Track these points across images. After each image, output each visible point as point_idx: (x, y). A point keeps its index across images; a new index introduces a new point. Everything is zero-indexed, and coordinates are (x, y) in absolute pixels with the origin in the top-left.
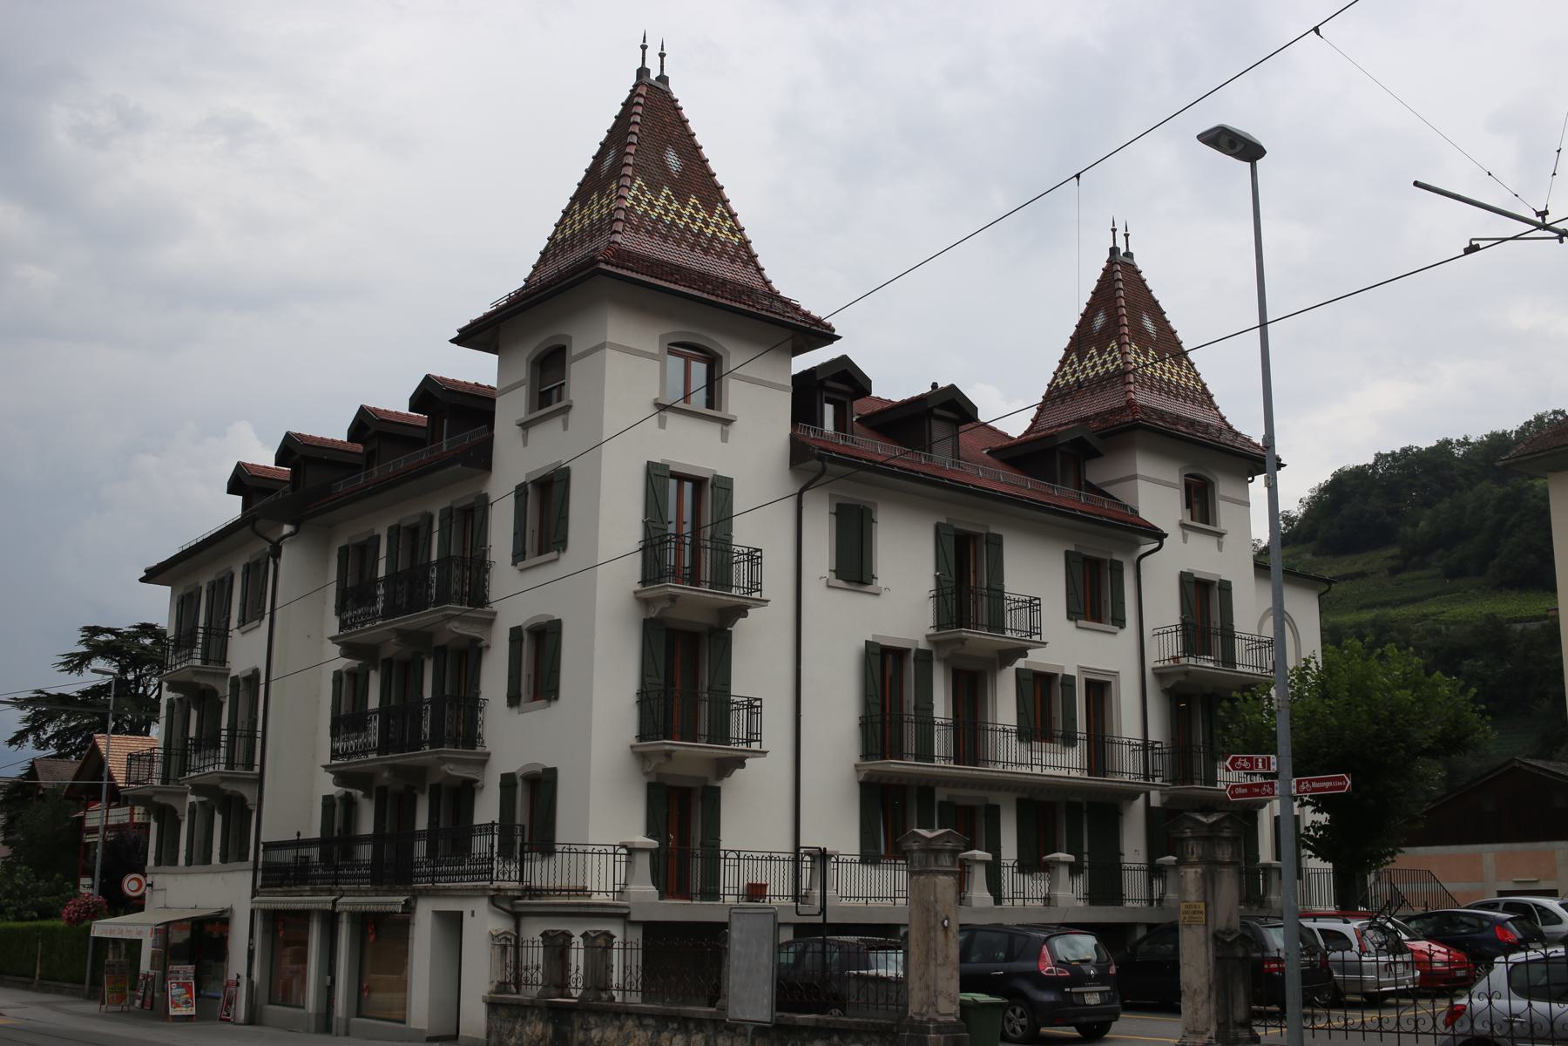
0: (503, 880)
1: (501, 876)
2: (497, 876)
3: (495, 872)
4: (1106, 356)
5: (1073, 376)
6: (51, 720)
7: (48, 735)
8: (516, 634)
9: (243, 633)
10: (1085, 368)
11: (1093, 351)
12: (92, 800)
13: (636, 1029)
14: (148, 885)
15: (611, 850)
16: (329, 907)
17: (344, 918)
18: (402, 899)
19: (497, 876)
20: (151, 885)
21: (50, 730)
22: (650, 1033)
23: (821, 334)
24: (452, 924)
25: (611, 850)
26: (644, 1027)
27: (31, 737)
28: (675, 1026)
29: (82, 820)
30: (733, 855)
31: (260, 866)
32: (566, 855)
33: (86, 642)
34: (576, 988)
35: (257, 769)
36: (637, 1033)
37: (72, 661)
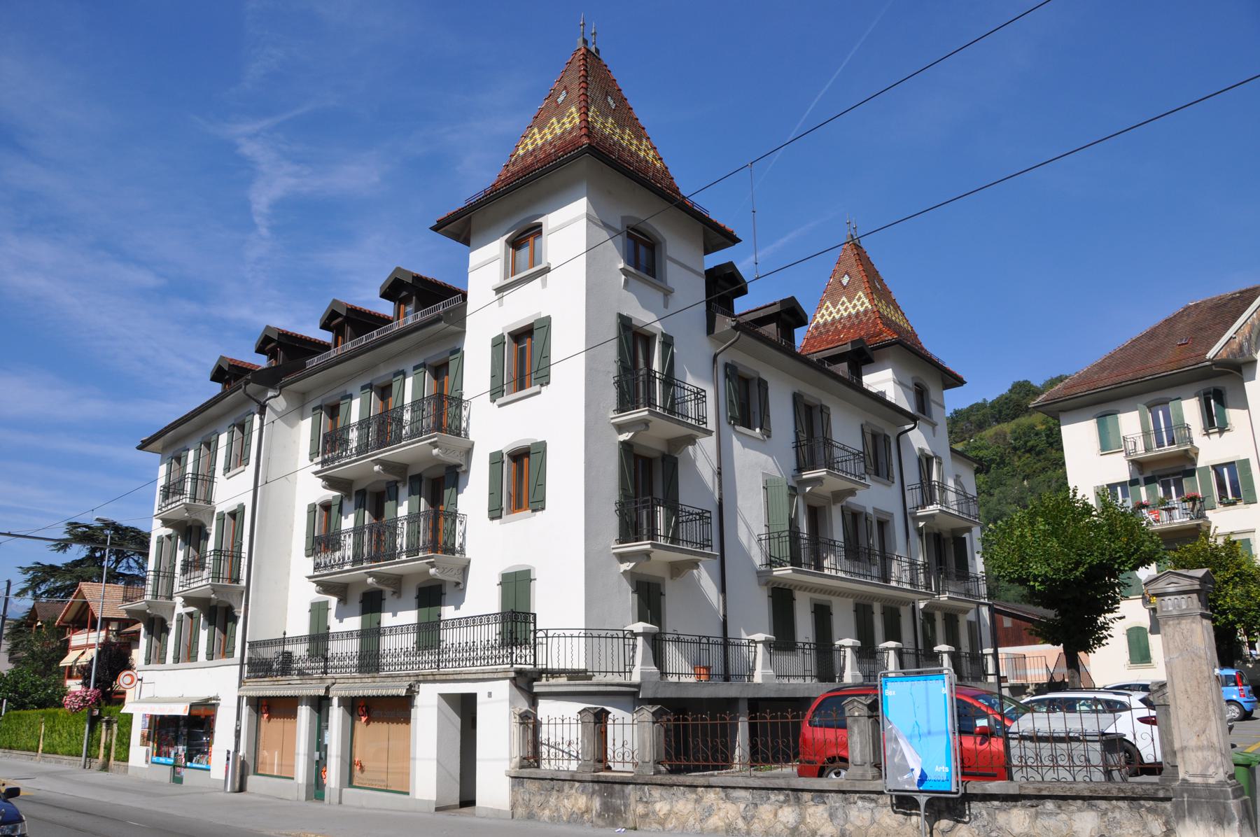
0: (521, 664)
1: (519, 659)
2: (516, 660)
3: (514, 655)
4: (855, 301)
5: (830, 316)
6: (44, 581)
7: (42, 591)
8: (496, 460)
9: (228, 479)
10: (839, 310)
11: (844, 299)
12: (77, 627)
13: (722, 801)
14: (139, 680)
15: (621, 634)
16: (322, 692)
17: (335, 701)
18: (406, 684)
19: (516, 660)
20: (141, 680)
21: (43, 588)
22: (742, 806)
23: (730, 239)
24: (465, 707)
25: (621, 634)
26: (734, 801)
27: (30, 593)
28: (782, 798)
29: (68, 641)
30: (704, 640)
31: (246, 661)
32: (569, 640)
33: (69, 532)
34: (624, 762)
35: (243, 583)
36: (724, 806)
37: (59, 544)
